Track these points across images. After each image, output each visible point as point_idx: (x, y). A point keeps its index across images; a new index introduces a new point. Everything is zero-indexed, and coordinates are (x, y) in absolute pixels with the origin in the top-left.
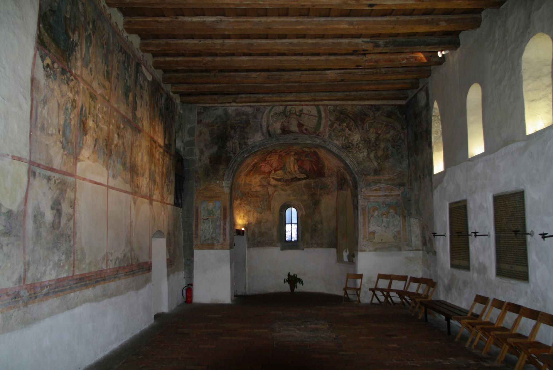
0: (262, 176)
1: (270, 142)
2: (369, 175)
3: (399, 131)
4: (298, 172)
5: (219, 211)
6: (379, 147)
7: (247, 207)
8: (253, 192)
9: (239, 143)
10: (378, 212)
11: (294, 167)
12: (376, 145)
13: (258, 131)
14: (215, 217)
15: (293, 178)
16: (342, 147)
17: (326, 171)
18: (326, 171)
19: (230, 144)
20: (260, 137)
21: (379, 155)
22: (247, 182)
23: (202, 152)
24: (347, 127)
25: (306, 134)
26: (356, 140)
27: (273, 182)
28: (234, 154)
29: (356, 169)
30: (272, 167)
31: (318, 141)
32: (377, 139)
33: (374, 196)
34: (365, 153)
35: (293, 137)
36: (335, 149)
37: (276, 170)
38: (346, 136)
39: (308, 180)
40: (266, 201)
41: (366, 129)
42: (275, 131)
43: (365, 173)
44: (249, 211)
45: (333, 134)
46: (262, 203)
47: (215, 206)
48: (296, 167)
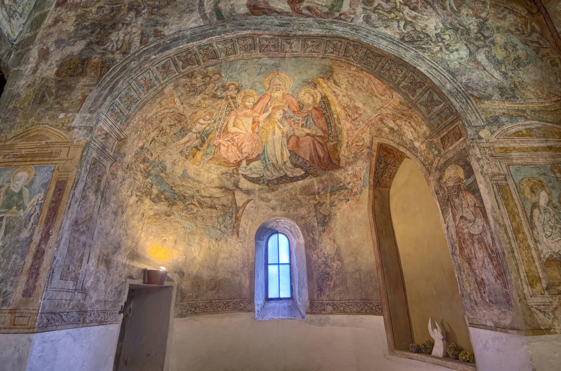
0: (224, 169)
1: (219, 29)
2: (489, 98)
3: (525, 17)
4: (289, 164)
5: (42, 195)
6: (493, 42)
7: (186, 223)
8: (204, 197)
9: (142, 33)
10: (549, 194)
11: (282, 154)
12: (485, 38)
13: (192, 11)
14: (22, 213)
15: (281, 177)
16: (403, 39)
17: (342, 152)
18: (344, 152)
19: (117, 37)
20: (195, 21)
21: (500, 58)
22: (191, 174)
23: (44, 55)
24: (406, 5)
25: (308, 16)
26: (432, 26)
27: (245, 184)
28: (124, 53)
29: (448, 86)
30: (242, 153)
31: (341, 29)
32: (482, 26)
33: (519, 150)
34: (464, 53)
35: (277, 22)
36: (385, 43)
37: (249, 161)
38: (405, 20)
39: (307, 181)
40: (231, 217)
41: (451, 8)
42: (233, 9)
43: (475, 94)
44: (192, 233)
45: (374, 16)
46: (221, 220)
47: (32, 182)
48: (287, 154)
